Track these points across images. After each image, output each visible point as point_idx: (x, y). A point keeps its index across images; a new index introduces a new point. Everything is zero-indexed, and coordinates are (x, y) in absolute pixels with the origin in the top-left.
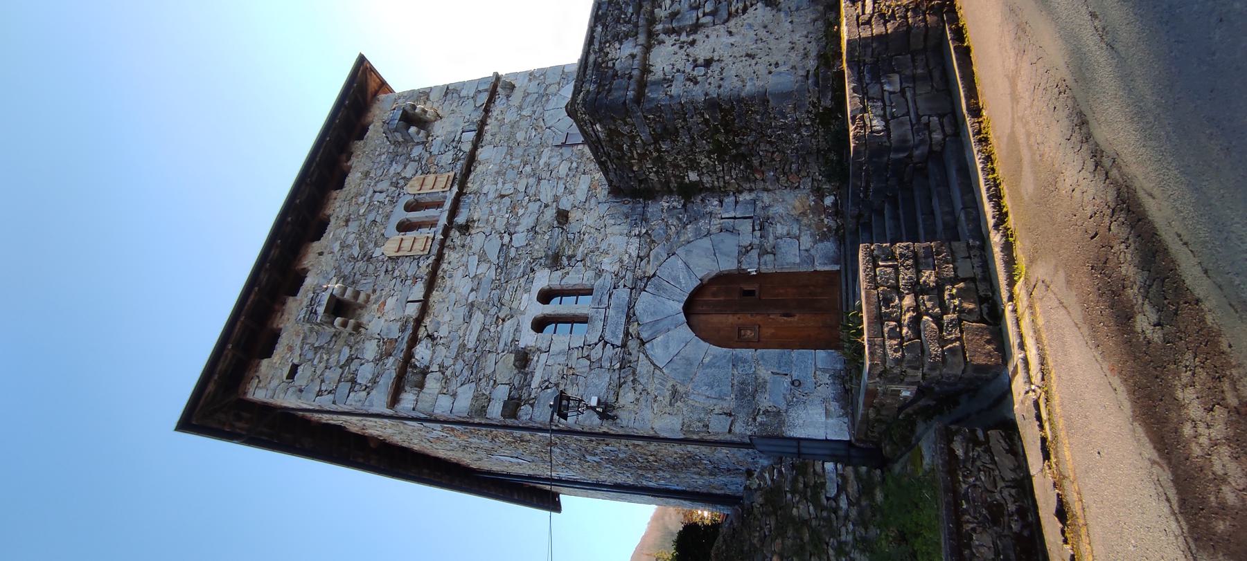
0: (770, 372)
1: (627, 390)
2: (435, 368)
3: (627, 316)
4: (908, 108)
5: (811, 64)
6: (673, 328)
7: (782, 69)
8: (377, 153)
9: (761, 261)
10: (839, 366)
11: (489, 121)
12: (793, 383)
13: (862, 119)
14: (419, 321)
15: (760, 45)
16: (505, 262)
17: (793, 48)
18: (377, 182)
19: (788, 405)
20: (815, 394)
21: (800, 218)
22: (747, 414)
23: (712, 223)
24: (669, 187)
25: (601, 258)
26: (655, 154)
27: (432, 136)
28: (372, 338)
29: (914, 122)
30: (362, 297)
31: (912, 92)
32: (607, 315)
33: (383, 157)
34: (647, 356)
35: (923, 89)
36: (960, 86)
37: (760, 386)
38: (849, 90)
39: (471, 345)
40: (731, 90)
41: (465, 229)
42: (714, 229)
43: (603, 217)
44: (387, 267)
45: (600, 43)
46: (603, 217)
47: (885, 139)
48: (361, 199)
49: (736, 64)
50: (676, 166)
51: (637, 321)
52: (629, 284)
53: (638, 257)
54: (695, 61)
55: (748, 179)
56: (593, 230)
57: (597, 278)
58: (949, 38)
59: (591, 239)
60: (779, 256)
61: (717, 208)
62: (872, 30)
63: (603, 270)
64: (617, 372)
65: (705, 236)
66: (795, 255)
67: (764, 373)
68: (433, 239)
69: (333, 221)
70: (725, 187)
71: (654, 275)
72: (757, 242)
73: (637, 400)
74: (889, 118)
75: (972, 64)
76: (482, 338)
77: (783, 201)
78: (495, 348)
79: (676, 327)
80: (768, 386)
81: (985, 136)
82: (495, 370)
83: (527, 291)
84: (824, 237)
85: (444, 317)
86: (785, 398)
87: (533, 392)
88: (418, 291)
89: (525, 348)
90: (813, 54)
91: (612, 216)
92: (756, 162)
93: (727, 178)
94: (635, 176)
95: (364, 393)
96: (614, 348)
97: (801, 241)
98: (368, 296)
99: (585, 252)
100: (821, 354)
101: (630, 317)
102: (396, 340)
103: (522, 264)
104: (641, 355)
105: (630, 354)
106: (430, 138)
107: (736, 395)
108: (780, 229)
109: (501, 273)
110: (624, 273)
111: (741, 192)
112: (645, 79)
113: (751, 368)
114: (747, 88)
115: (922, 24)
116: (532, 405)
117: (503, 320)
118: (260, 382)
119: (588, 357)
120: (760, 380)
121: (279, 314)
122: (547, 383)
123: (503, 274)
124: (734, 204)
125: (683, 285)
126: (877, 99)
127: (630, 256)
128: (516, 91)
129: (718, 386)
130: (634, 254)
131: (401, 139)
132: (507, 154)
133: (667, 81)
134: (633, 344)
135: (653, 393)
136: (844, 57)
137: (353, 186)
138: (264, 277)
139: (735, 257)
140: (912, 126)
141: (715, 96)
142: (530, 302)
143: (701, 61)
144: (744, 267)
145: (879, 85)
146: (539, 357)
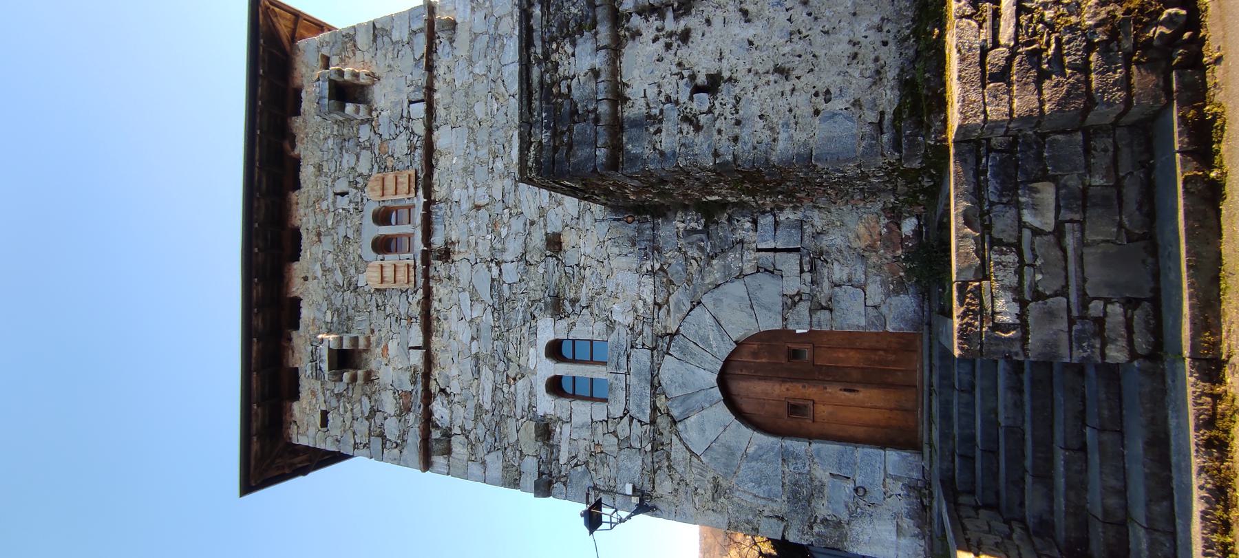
0: (828, 473)
1: (663, 477)
2: (456, 430)
3: (652, 385)
4: (1067, 277)
5: (888, 97)
6: (708, 405)
7: (838, 105)
8: (322, 137)
9: (814, 319)
10: (915, 475)
11: (437, 85)
12: (856, 490)
13: (978, 292)
14: (427, 376)
15: (799, 46)
17: (855, 56)
18: (334, 181)
19: (851, 516)
20: (885, 506)
21: (866, 254)
22: (802, 522)
23: (744, 258)
25: (610, 303)
27: (376, 110)
28: (385, 389)
29: (1075, 313)
31: (1078, 234)
32: (628, 382)
33: (330, 142)
34: (681, 440)
35: (1101, 230)
36: (1186, 294)
37: (817, 490)
38: (956, 216)
39: (487, 406)
40: (755, 148)
41: (446, 254)
42: (748, 269)
43: (604, 241)
44: (377, 301)
45: (543, 41)
46: (604, 241)
47: (1017, 348)
48: (324, 205)
49: (759, 90)
51: (664, 393)
52: (649, 343)
53: (655, 303)
54: (693, 77)
56: (595, 263)
57: (610, 332)
58: (1177, 147)
59: (594, 275)
60: (837, 313)
61: (751, 233)
62: (1010, 102)
63: (615, 321)
64: (649, 455)
65: (737, 278)
66: (859, 313)
67: (821, 473)
68: (415, 267)
71: (678, 332)
72: (806, 289)
73: (676, 490)
74: (1027, 297)
75: (1220, 235)
76: (497, 399)
77: (843, 225)
78: (513, 413)
79: (711, 406)
80: (826, 491)
81: (1221, 435)
82: (518, 439)
83: (533, 344)
84: (900, 287)
86: (847, 506)
87: (563, 470)
88: (417, 337)
89: (545, 416)
90: (891, 74)
91: (615, 242)
95: (396, 451)
96: (642, 425)
97: (867, 293)
98: (368, 339)
99: (590, 294)
100: (892, 456)
101: (655, 387)
102: (411, 393)
103: (519, 306)
104: (674, 437)
105: (661, 434)
106: (374, 114)
107: (788, 498)
108: (839, 272)
109: (499, 319)
110: (640, 327)
111: (782, 209)
112: (620, 114)
113: (804, 467)
114: (781, 145)
115: (1119, 95)
116: (565, 484)
117: (515, 379)
118: (298, 427)
119: (615, 433)
120: (816, 483)
121: (290, 352)
122: (575, 461)
123: (502, 320)
124: (773, 228)
125: (715, 350)
126: (1008, 245)
127: (645, 302)
128: (459, 26)
129: (766, 484)
130: (650, 300)
133: (652, 120)
134: (663, 422)
135: (693, 484)
136: (956, 335)
137: (311, 186)
138: (258, 322)
139: (779, 313)
140: (1071, 322)
141: (730, 158)
142: (538, 360)
143: (701, 80)
144: (790, 327)
145: (1013, 212)
146: (561, 428)
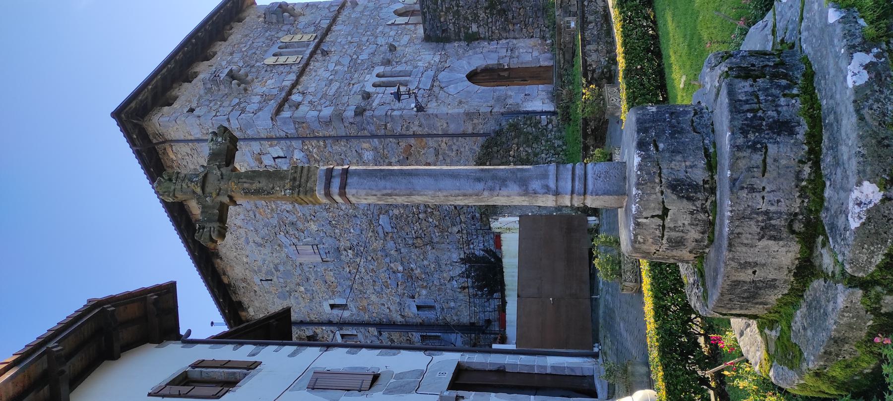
16: (354, 65)
24: (459, 36)
26: (455, 8)
30: (249, 78)
41: (325, 53)
50: (466, 19)
55: (505, 29)
69: (219, 54)
70: (492, 36)
85: (310, 83)
92: (510, 16)
93: (494, 28)
94: (441, 26)
95: (253, 114)
106: (296, 22)
111: (501, 39)
117: (353, 85)
130: (437, 61)
131: (274, 21)
132: (354, 28)
134: (436, 89)
